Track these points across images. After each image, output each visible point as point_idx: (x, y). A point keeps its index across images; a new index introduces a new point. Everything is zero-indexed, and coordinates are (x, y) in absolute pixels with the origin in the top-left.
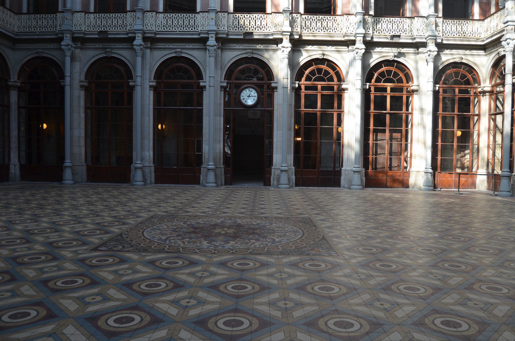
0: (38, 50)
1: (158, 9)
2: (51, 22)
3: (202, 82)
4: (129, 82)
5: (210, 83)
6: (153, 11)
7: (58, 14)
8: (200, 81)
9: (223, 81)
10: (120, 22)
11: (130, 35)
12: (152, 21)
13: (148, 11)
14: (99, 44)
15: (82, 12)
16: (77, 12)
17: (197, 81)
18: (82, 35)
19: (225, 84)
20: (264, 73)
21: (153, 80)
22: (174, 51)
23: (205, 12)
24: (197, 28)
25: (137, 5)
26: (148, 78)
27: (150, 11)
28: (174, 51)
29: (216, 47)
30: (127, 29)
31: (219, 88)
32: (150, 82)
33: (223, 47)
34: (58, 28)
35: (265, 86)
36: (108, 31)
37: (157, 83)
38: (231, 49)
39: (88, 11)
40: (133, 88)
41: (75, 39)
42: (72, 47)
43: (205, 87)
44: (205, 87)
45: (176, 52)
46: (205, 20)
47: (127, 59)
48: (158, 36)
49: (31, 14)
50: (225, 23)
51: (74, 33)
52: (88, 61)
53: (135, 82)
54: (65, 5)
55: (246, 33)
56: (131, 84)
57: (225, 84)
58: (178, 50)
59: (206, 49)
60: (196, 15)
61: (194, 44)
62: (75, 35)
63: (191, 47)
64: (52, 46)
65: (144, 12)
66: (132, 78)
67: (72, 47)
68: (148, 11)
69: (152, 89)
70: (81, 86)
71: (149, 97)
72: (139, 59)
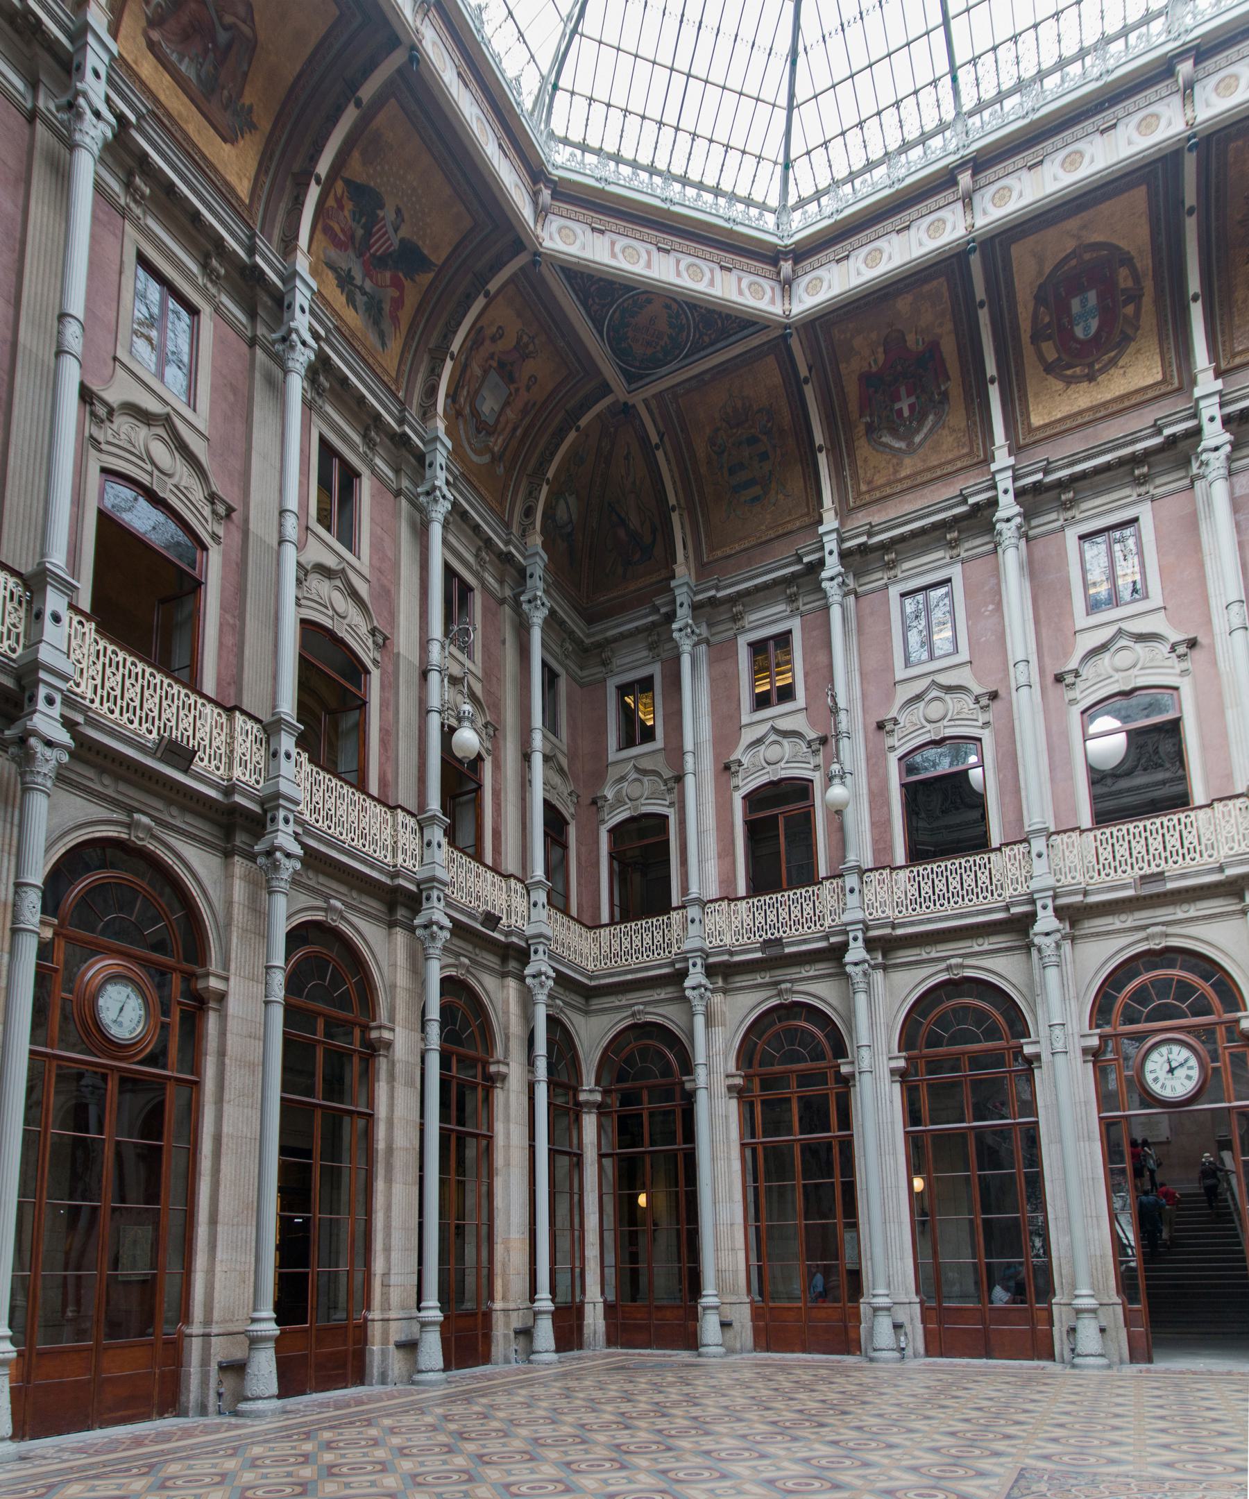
0: (636, 1008)
1: (893, 859)
2: (658, 937)
3: (1027, 1043)
4: (839, 1066)
5: (1056, 1045)
6: (883, 868)
7: (674, 914)
8: (1023, 1041)
9: (1087, 1031)
10: (808, 909)
11: (833, 940)
12: (883, 895)
13: (870, 870)
14: (763, 974)
15: (722, 899)
16: (711, 901)
17: (1013, 1042)
18: (726, 957)
19: (1095, 1042)
20: (1209, 989)
21: (896, 1053)
22: (943, 965)
23: (1015, 843)
24: (1000, 891)
25: (845, 857)
26: (885, 1049)
27: (876, 869)
28: (943, 965)
29: (1058, 936)
30: (826, 925)
31: (1079, 1053)
32: (890, 1059)
33: (1077, 933)
34: (675, 950)
35: (1221, 1032)
36: (781, 938)
37: (907, 1059)
38: (1098, 934)
39: (733, 896)
40: (846, 1081)
41: (711, 971)
42: (706, 989)
43: (1037, 1057)
44: (1037, 1057)
45: (949, 968)
46: (1017, 864)
47: (829, 1005)
48: (900, 932)
49: (617, 923)
50: (1076, 861)
51: (708, 955)
52: (742, 1022)
53: (852, 1063)
54: (685, 890)
55: (1142, 877)
56: (844, 1069)
57: (1095, 1042)
58: (953, 961)
59: (1028, 947)
60: (993, 856)
61: (994, 939)
62: (711, 960)
63: (986, 947)
64: (662, 994)
65: (862, 872)
66: (845, 1055)
67: (706, 989)
68: (870, 870)
69: (898, 1078)
70: (730, 1088)
71: (891, 1102)
72: (861, 999)
